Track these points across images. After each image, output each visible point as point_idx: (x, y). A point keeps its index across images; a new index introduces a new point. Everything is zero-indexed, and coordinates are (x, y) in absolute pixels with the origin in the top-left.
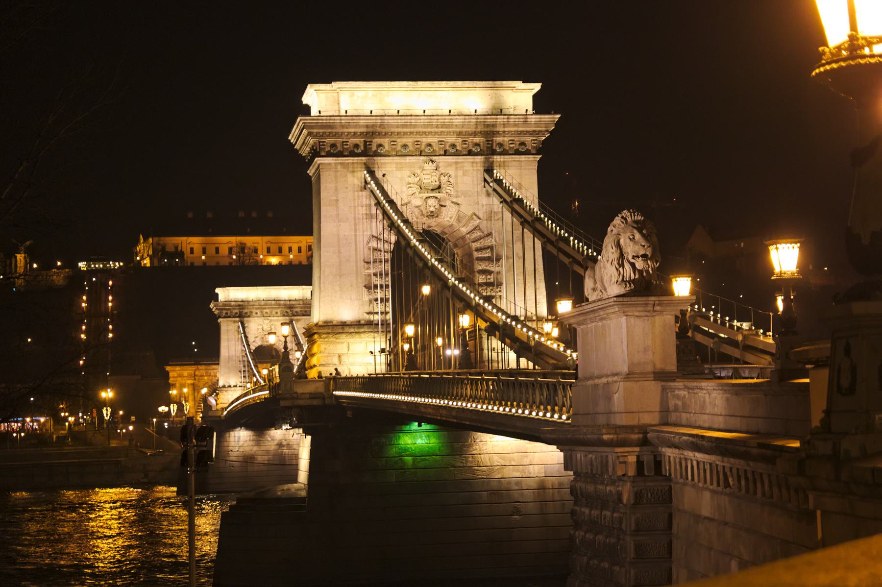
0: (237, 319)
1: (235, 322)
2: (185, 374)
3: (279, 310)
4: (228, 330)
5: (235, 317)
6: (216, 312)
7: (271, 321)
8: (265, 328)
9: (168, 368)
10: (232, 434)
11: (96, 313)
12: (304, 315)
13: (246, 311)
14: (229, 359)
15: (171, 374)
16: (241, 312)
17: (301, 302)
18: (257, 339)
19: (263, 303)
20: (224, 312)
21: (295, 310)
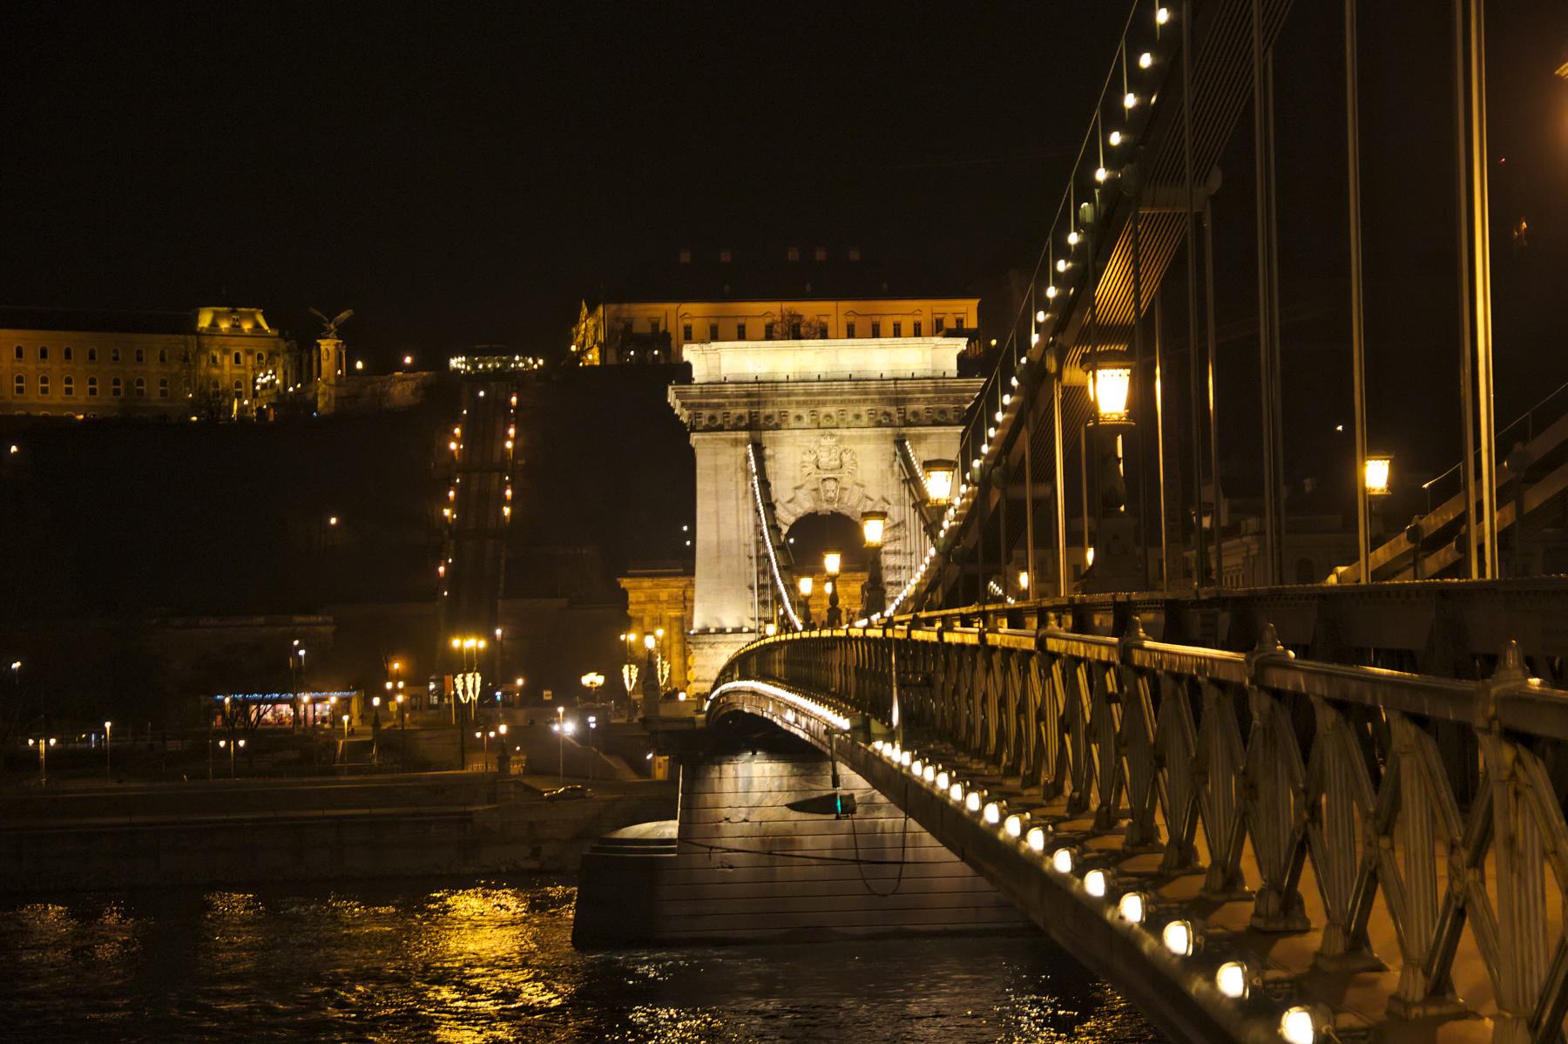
0: (744, 435)
1: (736, 443)
2: (664, 595)
3: (863, 409)
4: (718, 467)
5: (736, 428)
6: (685, 416)
7: (841, 440)
8: (824, 460)
9: (625, 583)
10: (729, 769)
11: (482, 462)
12: (936, 424)
13: (769, 411)
14: (720, 550)
15: (632, 597)
16: (755, 413)
17: (929, 384)
18: (801, 494)
19: (816, 387)
20: (706, 413)
21: (912, 407)
